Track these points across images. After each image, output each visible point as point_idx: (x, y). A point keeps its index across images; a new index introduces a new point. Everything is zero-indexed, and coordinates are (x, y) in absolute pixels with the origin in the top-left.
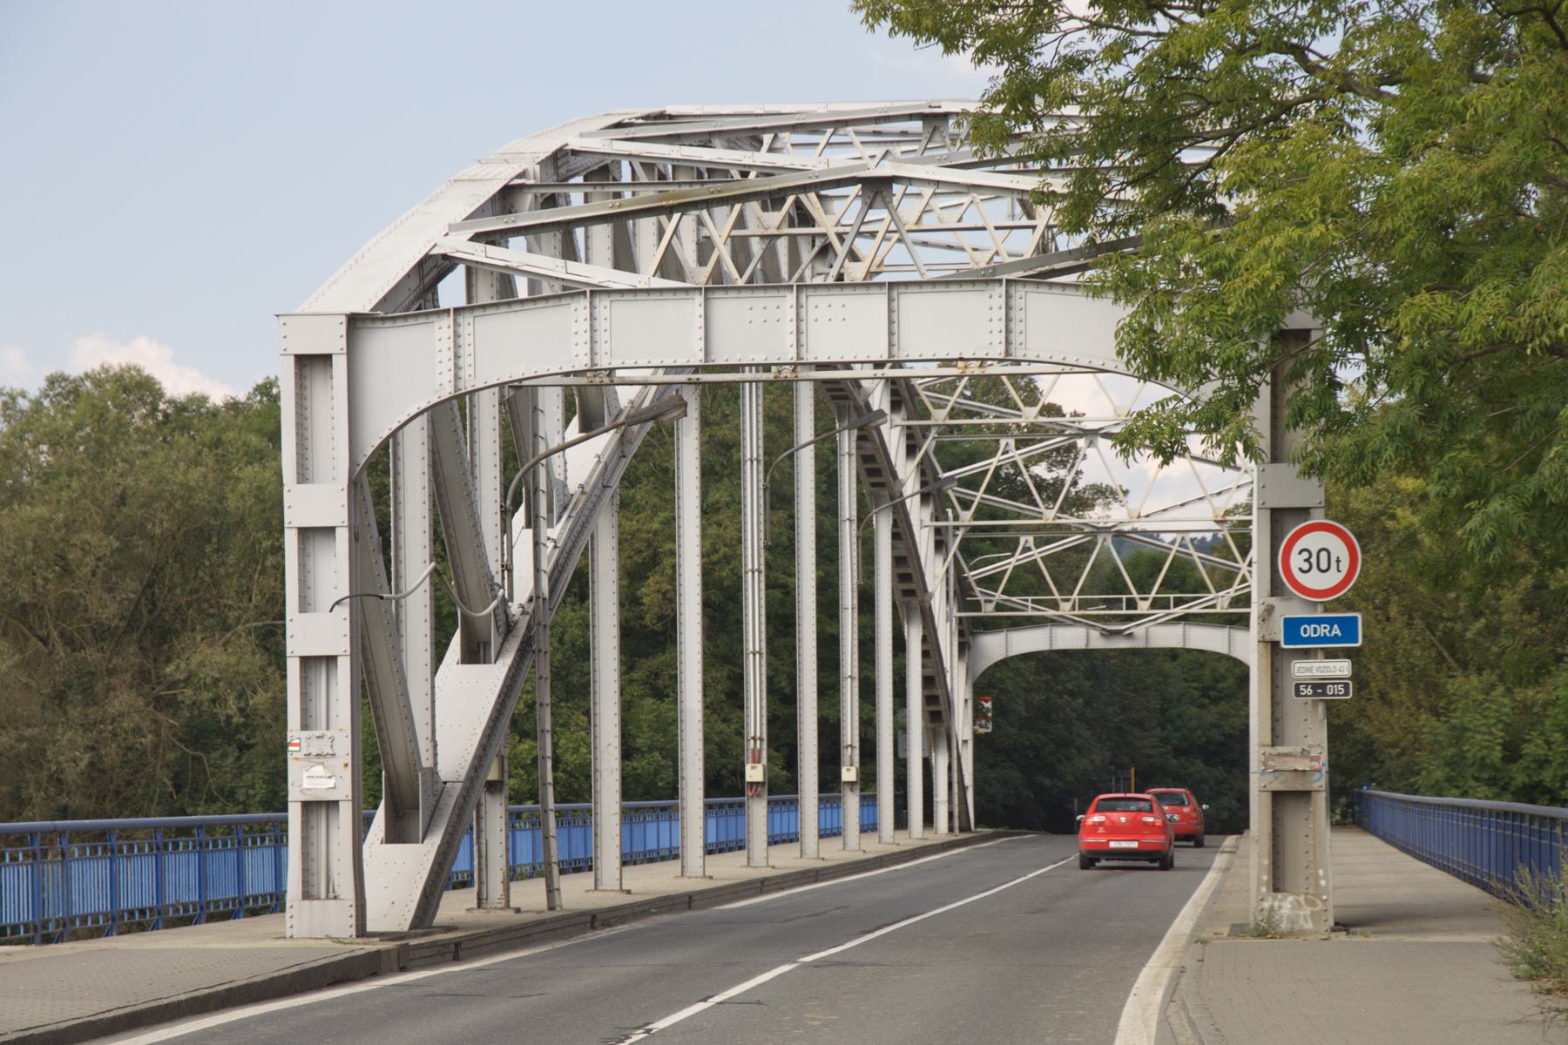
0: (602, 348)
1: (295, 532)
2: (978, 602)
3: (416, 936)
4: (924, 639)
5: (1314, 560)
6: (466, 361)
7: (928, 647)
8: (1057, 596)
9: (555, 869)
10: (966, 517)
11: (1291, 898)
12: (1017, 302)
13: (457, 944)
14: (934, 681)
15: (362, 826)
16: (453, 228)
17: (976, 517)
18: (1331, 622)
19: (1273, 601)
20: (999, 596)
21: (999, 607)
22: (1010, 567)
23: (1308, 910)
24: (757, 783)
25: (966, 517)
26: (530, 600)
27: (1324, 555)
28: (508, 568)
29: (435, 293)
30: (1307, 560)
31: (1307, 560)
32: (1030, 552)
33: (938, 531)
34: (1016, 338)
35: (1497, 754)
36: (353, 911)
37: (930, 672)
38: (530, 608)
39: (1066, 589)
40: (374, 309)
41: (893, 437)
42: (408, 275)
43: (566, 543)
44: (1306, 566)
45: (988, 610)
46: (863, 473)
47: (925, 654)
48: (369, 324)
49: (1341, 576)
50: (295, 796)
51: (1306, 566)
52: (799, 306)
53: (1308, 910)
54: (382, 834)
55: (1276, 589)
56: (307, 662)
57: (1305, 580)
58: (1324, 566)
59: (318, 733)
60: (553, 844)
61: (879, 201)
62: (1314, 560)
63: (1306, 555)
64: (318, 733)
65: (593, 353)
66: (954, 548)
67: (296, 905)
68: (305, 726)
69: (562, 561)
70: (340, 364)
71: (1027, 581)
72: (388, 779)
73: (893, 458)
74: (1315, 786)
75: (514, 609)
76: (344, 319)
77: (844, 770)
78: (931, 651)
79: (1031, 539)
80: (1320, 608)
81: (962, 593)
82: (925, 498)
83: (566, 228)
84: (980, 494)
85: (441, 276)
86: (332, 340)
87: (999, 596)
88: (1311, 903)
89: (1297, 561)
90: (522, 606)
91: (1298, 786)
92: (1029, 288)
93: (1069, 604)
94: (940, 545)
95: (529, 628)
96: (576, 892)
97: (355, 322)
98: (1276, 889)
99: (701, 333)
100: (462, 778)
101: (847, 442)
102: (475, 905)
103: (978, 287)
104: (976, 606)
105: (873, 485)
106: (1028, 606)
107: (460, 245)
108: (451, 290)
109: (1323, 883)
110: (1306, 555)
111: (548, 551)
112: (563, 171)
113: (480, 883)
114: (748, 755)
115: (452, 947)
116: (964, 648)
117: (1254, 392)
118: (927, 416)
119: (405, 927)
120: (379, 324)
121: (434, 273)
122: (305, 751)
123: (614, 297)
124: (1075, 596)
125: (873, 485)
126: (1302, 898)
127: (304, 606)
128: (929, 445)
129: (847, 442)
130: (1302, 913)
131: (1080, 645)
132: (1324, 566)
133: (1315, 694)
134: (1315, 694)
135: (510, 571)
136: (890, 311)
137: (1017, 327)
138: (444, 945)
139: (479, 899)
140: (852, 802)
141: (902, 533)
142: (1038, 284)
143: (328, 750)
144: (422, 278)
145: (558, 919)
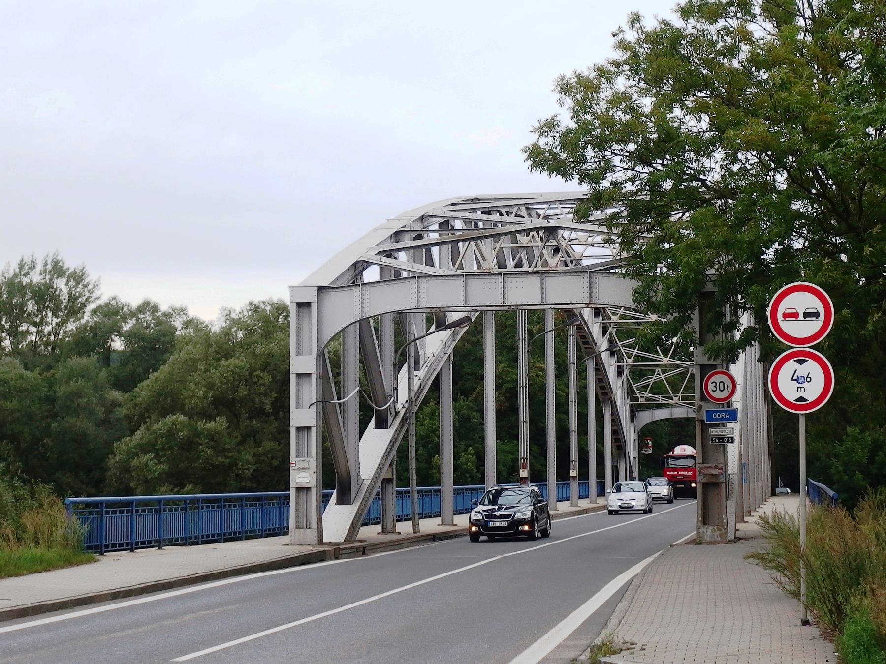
0: (422, 300)
1: (295, 375)
2: (638, 397)
3: (346, 544)
4: (612, 414)
5: (718, 386)
6: (366, 305)
7: (614, 417)
8: (672, 395)
9: (417, 517)
10: (630, 361)
11: (711, 528)
12: (595, 280)
13: (364, 548)
14: (617, 433)
15: (326, 499)
16: (369, 249)
17: (633, 361)
18: (725, 411)
19: (701, 403)
20: (647, 394)
21: (647, 399)
22: (651, 383)
23: (718, 533)
24: (525, 478)
25: (630, 361)
26: (407, 402)
27: (722, 384)
28: (396, 389)
29: (362, 275)
30: (715, 386)
31: (715, 386)
32: (659, 376)
33: (619, 367)
34: (594, 295)
35: (865, 460)
36: (316, 534)
37: (615, 428)
38: (406, 405)
39: (676, 391)
40: (330, 284)
41: (595, 330)
42: (349, 269)
43: (425, 378)
44: (714, 389)
45: (642, 401)
46: (581, 344)
47: (613, 420)
48: (327, 290)
49: (729, 393)
50: (293, 485)
51: (714, 389)
52: (504, 282)
53: (718, 533)
54: (335, 501)
55: (703, 398)
56: (299, 429)
57: (714, 394)
58: (722, 389)
59: (303, 459)
60: (416, 506)
61: (551, 237)
62: (718, 386)
63: (714, 384)
64: (303, 459)
65: (419, 301)
66: (626, 371)
67: (293, 530)
68: (297, 456)
69: (423, 385)
70: (314, 307)
71: (657, 389)
72: (338, 477)
73: (595, 339)
74: (721, 480)
75: (399, 406)
76: (316, 289)
77: (571, 471)
78: (615, 419)
79: (660, 370)
80: (721, 406)
81: (630, 393)
82: (612, 354)
83: (428, 247)
84: (636, 351)
85: (364, 270)
86: (311, 297)
87: (647, 394)
88: (720, 530)
89: (711, 387)
90: (402, 404)
91: (714, 480)
92: (599, 275)
93: (678, 398)
94: (620, 373)
95: (405, 414)
96: (429, 526)
97: (321, 289)
98: (705, 524)
99: (463, 293)
100: (371, 477)
101: (572, 330)
102: (380, 531)
103: (578, 274)
104: (637, 399)
105: (586, 348)
106: (660, 399)
107: (371, 256)
108: (371, 274)
109: (724, 521)
110: (714, 384)
111: (416, 383)
112: (425, 224)
113: (383, 522)
114: (521, 465)
115: (362, 549)
116: (633, 418)
117: (689, 319)
118: (610, 319)
119: (343, 541)
120: (330, 290)
121: (361, 268)
122: (297, 466)
123: (428, 279)
124: (680, 395)
125: (586, 348)
126: (716, 527)
127: (298, 406)
128: (612, 330)
129: (572, 330)
130: (716, 534)
131: (684, 416)
132: (722, 389)
133: (719, 442)
134: (719, 442)
135: (397, 390)
136: (542, 284)
137: (594, 290)
138: (357, 548)
139: (383, 528)
140: (575, 485)
141: (600, 369)
142: (603, 273)
143: (307, 466)
144: (355, 270)
145: (419, 537)
